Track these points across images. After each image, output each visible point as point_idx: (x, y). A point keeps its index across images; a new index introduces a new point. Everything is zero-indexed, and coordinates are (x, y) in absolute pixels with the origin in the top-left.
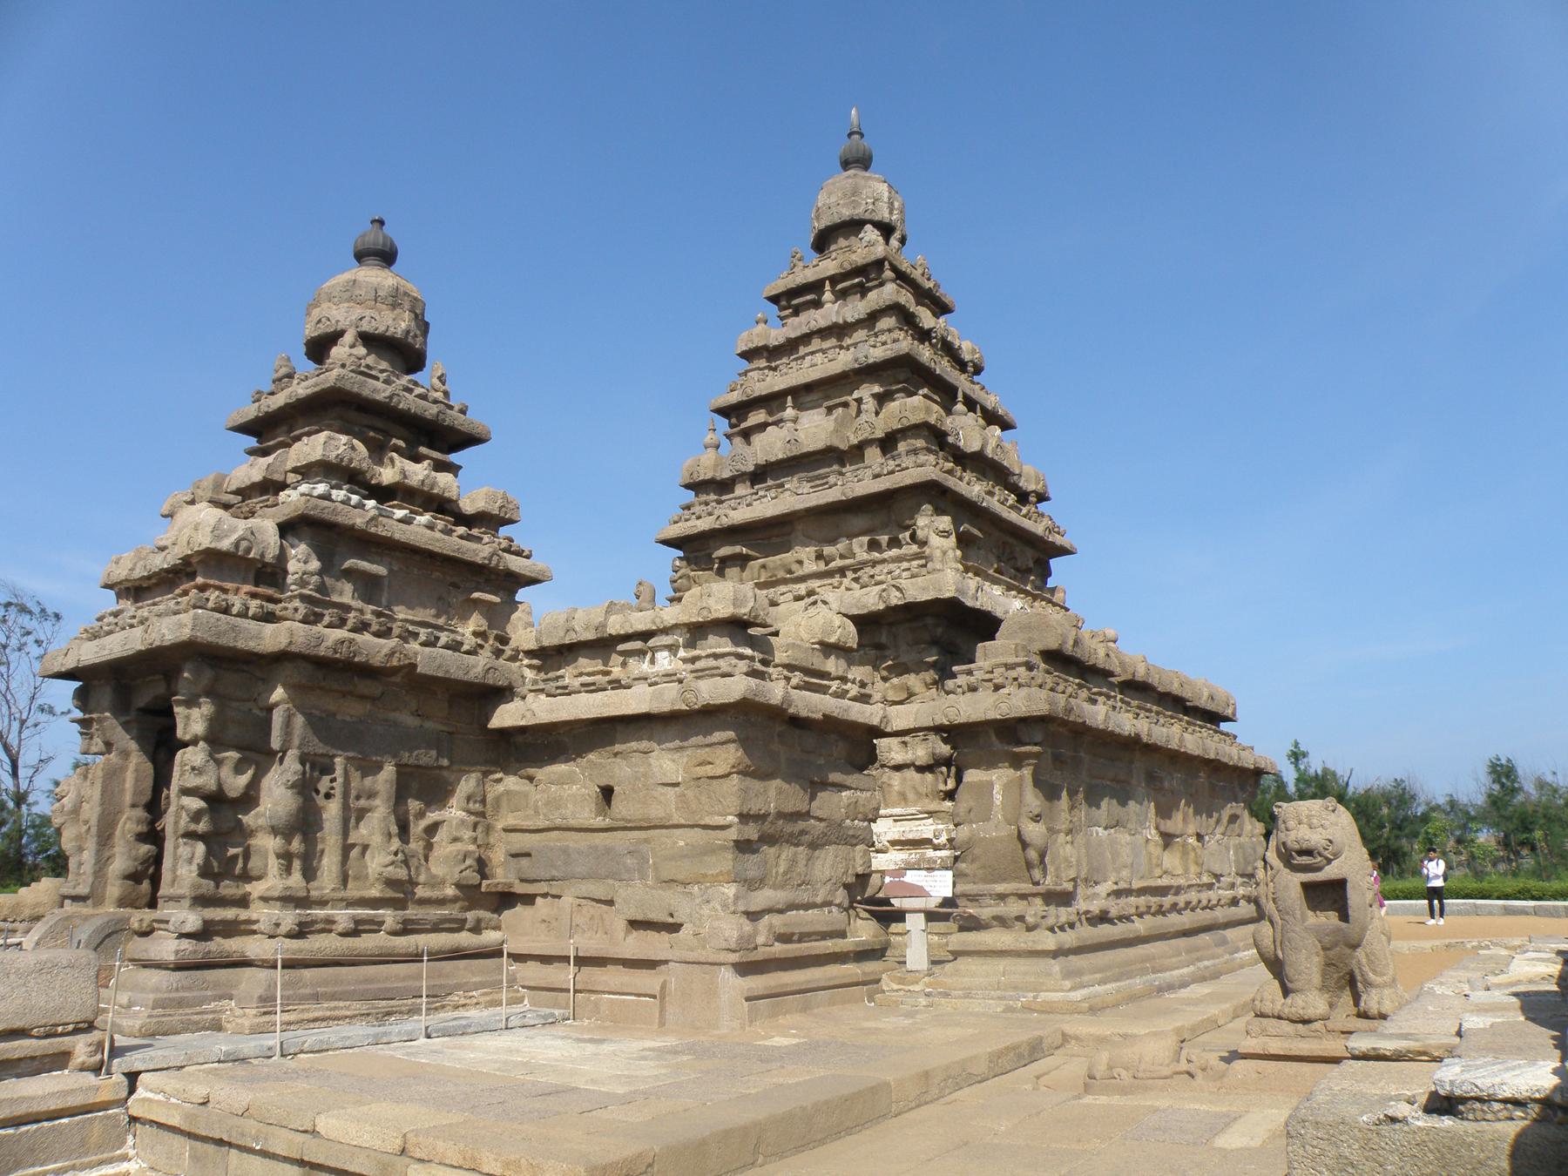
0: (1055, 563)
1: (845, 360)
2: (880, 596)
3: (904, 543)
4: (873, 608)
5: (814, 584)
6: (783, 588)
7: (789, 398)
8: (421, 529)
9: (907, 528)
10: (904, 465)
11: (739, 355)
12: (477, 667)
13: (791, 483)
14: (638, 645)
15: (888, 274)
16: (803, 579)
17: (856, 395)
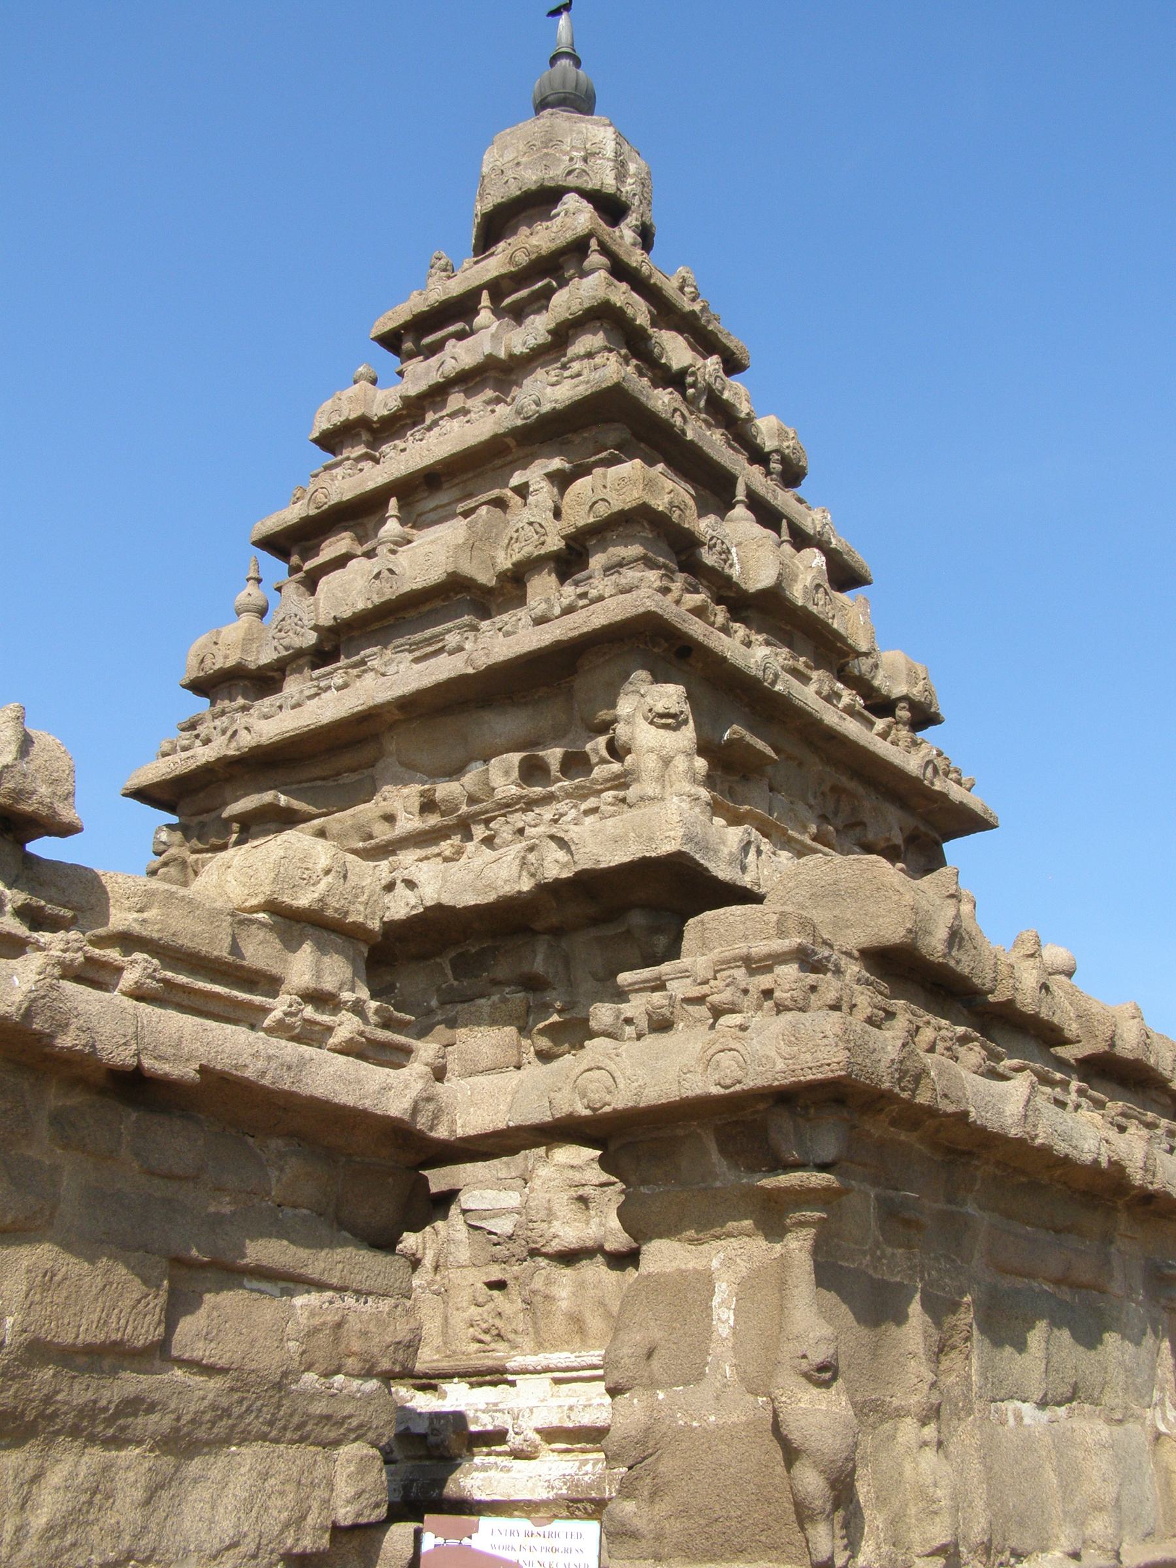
2: (524, 863)
3: (594, 759)
4: (508, 889)
7: (393, 501)
10: (593, 593)
11: (312, 441)
13: (375, 656)
15: (595, 258)
17: (516, 479)
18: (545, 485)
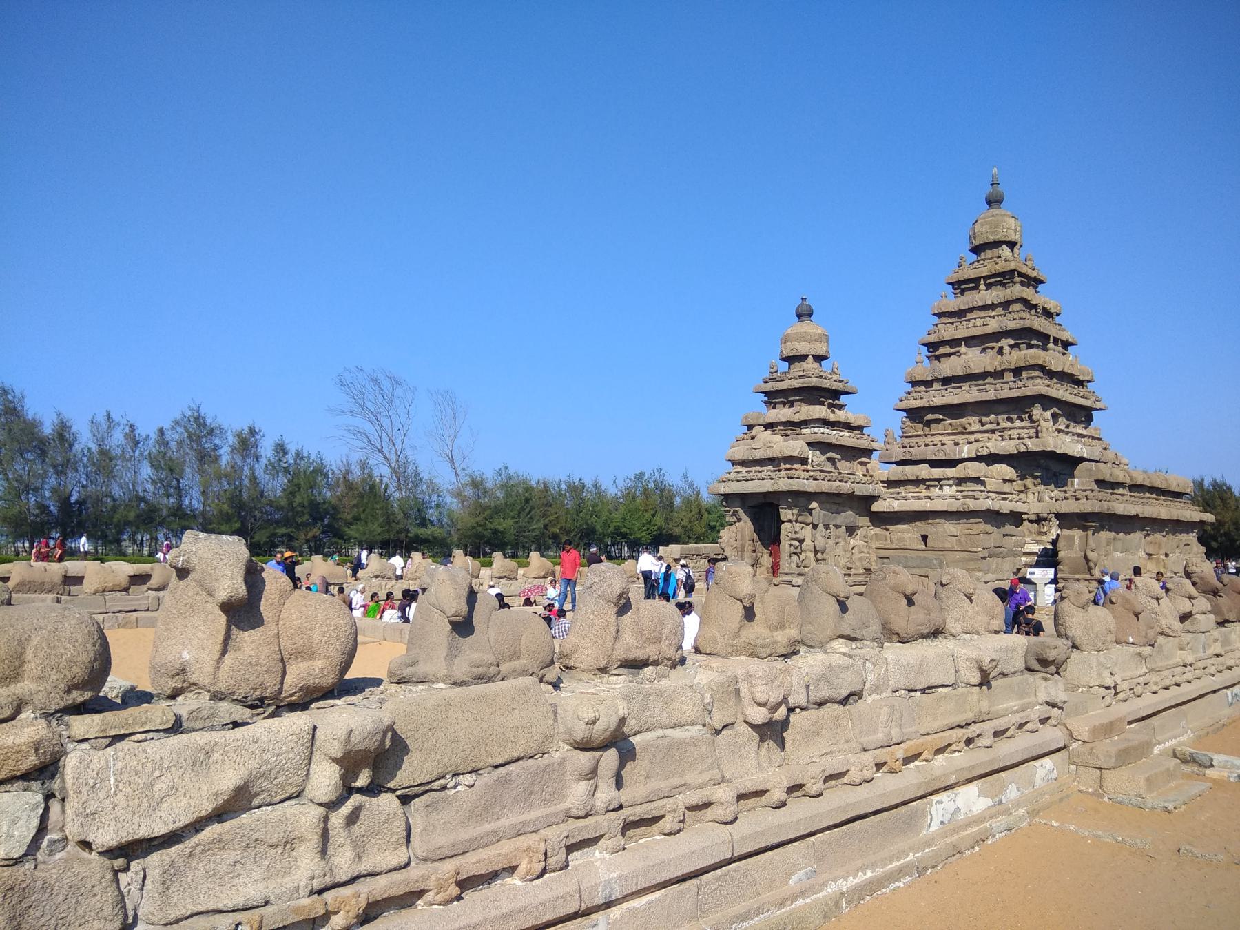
0: (1094, 413)
1: (993, 325)
4: (1012, 452)
5: (979, 436)
6: (963, 437)
8: (845, 438)
9: (1027, 413)
12: (870, 490)
13: (966, 386)
14: (936, 483)
16: (972, 433)
17: (999, 344)
18: (1008, 348)
